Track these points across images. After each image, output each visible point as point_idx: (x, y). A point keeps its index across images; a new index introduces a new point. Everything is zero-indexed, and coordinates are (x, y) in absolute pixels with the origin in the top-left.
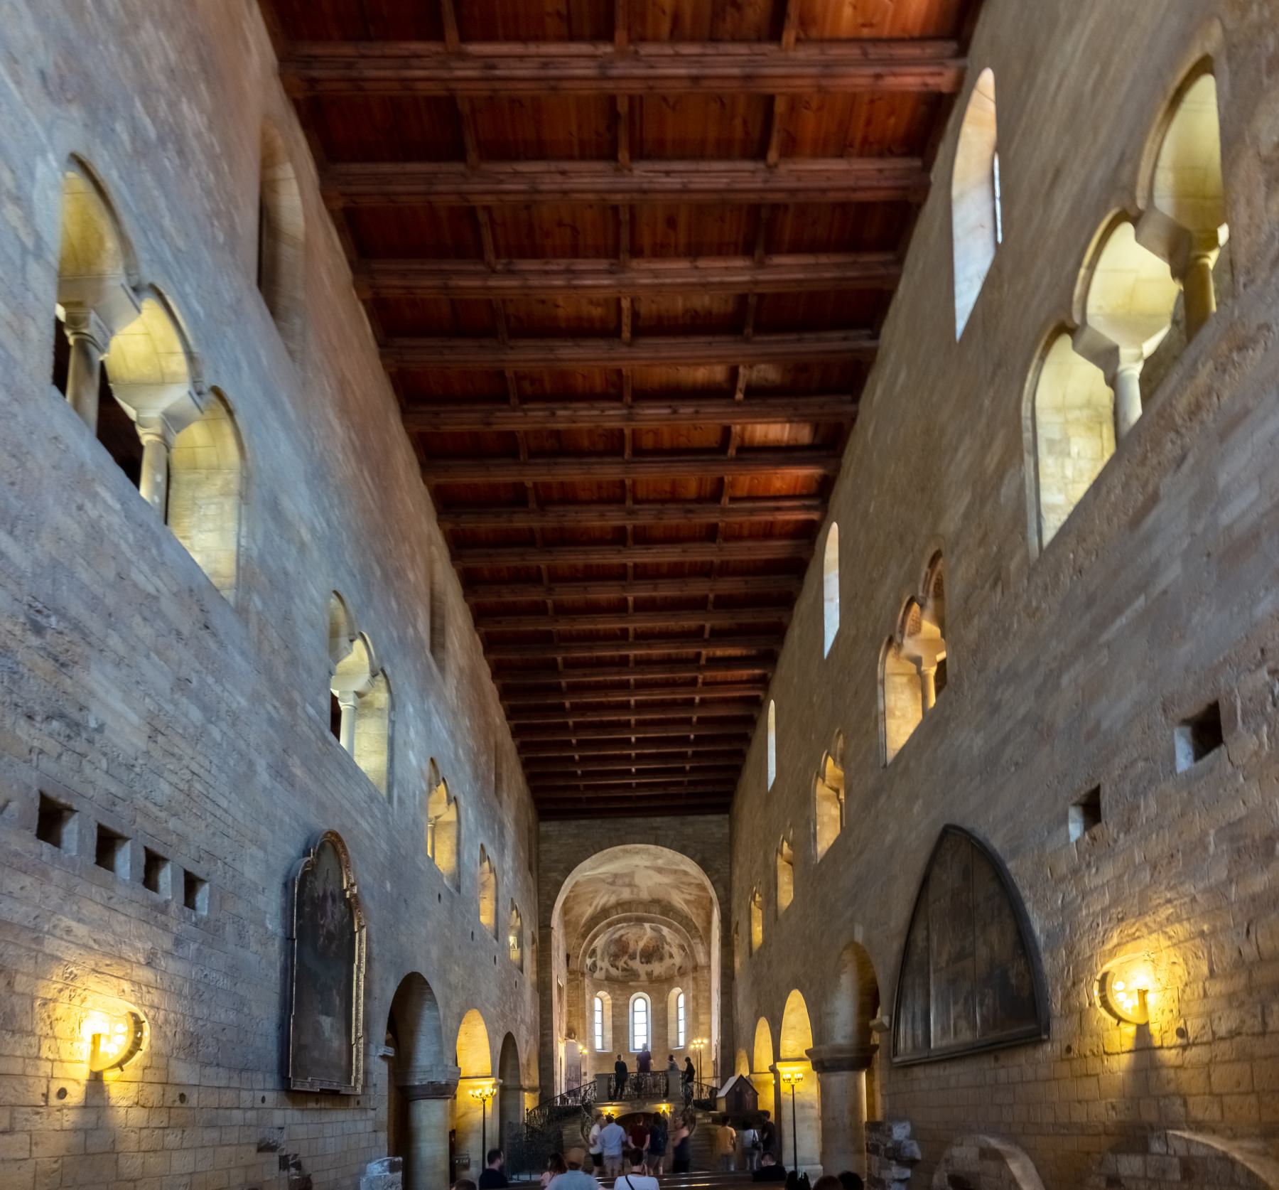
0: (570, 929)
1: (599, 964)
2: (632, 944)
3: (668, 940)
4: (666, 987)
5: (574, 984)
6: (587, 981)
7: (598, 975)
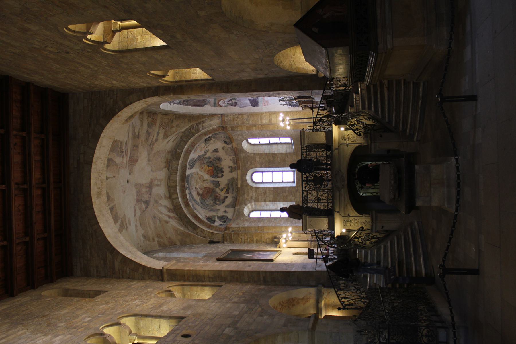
1: (220, 214)
2: (205, 185)
3: (202, 153)
4: (242, 155)
5: (234, 237)
6: (234, 225)
7: (230, 215)
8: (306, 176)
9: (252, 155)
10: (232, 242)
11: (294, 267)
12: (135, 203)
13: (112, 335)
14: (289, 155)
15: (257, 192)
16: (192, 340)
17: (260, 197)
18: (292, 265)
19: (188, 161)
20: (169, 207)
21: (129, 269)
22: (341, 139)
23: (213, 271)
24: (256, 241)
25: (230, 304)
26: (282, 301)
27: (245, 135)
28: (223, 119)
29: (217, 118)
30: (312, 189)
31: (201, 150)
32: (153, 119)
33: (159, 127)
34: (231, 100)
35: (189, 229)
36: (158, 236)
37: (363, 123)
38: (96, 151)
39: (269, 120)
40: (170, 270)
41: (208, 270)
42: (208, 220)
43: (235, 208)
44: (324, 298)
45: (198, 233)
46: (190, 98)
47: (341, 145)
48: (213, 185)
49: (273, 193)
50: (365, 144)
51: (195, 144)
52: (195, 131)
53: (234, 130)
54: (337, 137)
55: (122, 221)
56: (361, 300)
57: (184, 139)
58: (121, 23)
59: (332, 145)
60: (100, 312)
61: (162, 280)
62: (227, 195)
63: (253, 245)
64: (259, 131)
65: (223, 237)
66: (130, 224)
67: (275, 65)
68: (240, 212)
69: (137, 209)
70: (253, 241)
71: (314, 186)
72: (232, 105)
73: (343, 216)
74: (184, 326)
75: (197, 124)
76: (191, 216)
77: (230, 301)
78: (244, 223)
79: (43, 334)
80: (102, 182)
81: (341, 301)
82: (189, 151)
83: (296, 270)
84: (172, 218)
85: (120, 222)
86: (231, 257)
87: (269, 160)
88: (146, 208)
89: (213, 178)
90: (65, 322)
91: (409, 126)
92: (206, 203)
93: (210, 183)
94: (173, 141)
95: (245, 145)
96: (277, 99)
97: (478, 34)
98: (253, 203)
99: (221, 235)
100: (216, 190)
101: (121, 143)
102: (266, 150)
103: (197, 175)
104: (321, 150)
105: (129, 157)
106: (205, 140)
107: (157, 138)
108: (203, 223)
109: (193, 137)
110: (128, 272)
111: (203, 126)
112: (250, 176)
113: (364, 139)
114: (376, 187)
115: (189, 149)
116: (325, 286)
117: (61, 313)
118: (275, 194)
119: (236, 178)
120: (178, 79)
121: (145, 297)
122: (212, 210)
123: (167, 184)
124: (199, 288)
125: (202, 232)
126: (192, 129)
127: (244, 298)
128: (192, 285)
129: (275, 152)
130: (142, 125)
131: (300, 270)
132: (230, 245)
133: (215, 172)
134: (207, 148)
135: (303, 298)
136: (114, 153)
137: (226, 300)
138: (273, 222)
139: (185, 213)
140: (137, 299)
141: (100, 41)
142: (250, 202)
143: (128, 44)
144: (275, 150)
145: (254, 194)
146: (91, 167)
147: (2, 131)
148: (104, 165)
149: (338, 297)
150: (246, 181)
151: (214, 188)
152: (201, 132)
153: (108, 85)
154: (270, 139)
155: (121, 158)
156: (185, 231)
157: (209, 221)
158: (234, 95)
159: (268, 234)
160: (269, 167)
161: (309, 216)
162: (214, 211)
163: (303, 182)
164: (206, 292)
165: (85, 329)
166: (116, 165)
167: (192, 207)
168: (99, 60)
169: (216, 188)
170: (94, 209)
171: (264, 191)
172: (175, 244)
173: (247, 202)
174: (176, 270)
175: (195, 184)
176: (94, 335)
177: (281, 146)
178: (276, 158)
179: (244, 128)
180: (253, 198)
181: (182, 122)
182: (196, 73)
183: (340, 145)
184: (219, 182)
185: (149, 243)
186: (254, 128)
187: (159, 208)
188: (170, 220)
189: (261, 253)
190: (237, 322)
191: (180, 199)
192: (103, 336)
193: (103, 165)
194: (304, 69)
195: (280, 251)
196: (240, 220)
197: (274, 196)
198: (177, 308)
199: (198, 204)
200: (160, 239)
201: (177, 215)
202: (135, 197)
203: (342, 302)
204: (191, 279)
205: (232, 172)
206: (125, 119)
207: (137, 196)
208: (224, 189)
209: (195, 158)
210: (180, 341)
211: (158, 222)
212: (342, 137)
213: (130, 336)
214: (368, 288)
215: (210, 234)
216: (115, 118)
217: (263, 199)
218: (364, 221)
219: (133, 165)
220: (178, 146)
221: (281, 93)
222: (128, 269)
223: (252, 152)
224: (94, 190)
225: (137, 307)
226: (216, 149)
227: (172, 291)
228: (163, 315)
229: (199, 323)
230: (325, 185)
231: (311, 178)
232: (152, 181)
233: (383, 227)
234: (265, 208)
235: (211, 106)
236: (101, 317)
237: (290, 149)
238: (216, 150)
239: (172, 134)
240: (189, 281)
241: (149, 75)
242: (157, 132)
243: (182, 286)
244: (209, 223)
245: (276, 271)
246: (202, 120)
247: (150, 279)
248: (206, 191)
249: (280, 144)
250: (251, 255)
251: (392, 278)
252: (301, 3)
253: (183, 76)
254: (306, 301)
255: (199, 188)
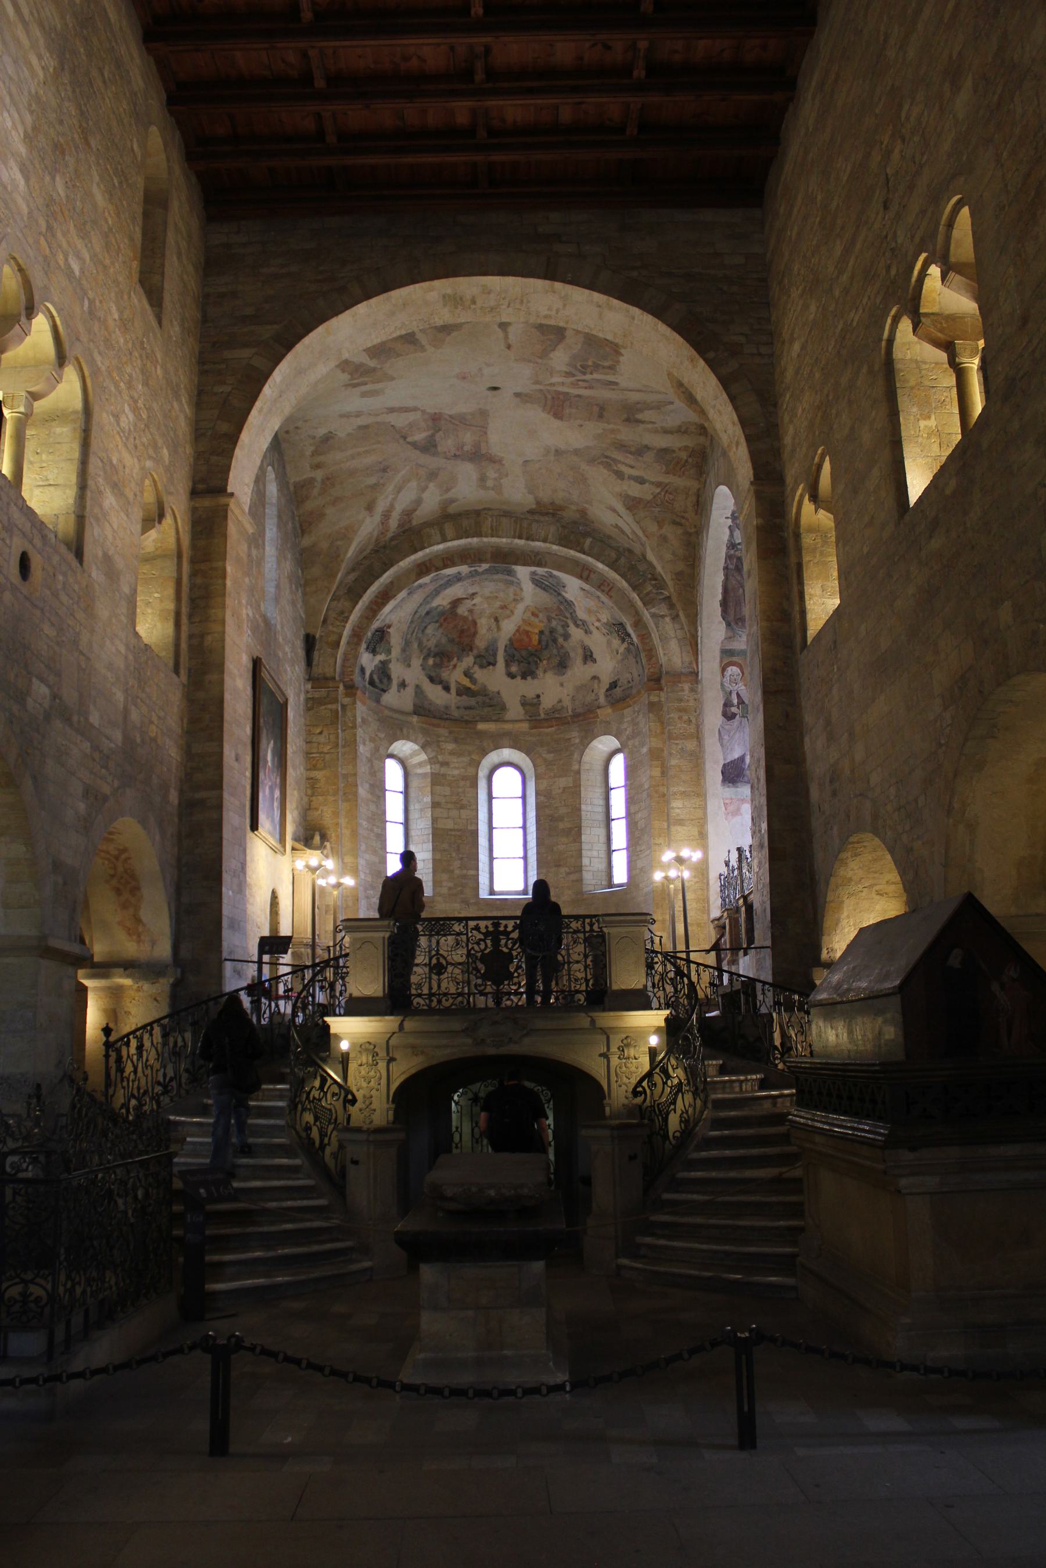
0: (316, 571)
1: (396, 670)
2: (484, 624)
3: (581, 614)
4: (575, 735)
5: (324, 710)
6: (361, 710)
7: (391, 698)
8: (510, 929)
9: (576, 767)
10: (312, 704)
11: (233, 892)
12: (428, 411)
13: (28, 339)
14: (573, 877)
15: (463, 780)
16: (12, 584)
17: (447, 791)
18: (242, 886)
19: (555, 573)
20: (417, 513)
21: (230, 392)
22: (625, 1036)
23: (223, 647)
24: (312, 778)
25: (122, 699)
26: (129, 858)
27: (637, 744)
28: (683, 678)
29: (688, 658)
30: (473, 948)
31: (589, 611)
32: (684, 466)
33: (658, 484)
34: (741, 702)
35: (348, 573)
36: (328, 479)
37: (671, 1103)
38: (587, 292)
39: (682, 817)
40: (226, 517)
41: (224, 632)
42: (377, 631)
43: (415, 713)
44: (140, 984)
45: (339, 600)
46: (749, 577)
47: (605, 1036)
48: (483, 647)
49: (458, 830)
50: (607, 1109)
51: (607, 594)
52: (648, 594)
53: (650, 711)
54: (629, 1025)
55: (374, 370)
56: (133, 1096)
57: (623, 560)
58: (975, 367)
59: (604, 1010)
60: (98, 303)
61: (194, 493)
62: (453, 691)
63: (302, 768)
64: (646, 786)
65: (326, 679)
66: (364, 395)
67: (848, 837)
68: (401, 730)
69: (412, 417)
70: (314, 768)
71: (479, 955)
72: (727, 704)
73: (391, 1042)
74: (56, 559)
75: (668, 598)
76: (388, 581)
77: (130, 698)
78: (367, 743)
79: (30, 130)
80: (492, 309)
81: (131, 1037)
82: (585, 574)
83: (225, 901)
84: (383, 523)
85: (372, 363)
86: (264, 701)
87: (561, 819)
88: (415, 445)
89: (506, 646)
90: (67, 196)
91: (662, 1242)
92: (429, 627)
93: (490, 637)
94: (617, 526)
95: (605, 743)
96: (746, 841)
97: (942, 1452)
98: (427, 769)
99: (332, 670)
100: (468, 655)
101: (610, 368)
102: (591, 808)
103: (515, 600)
104: (589, 977)
105: (567, 393)
106: (621, 624)
107: (626, 476)
108: (367, 618)
109: (630, 585)
110: (219, 389)
111: (663, 616)
112: (511, 760)
113: (624, 1105)
114: (477, 1142)
115: (592, 576)
116: (175, 986)
117: (95, 185)
118: (455, 836)
119: (506, 719)
120: (807, 540)
121: (144, 440)
122: (407, 644)
123: (487, 506)
124: (171, 606)
125: (342, 613)
126: (654, 582)
127: (138, 740)
128: (179, 583)
129: (583, 837)
130: (666, 431)
131: (226, 911)
132: (302, 697)
133: (524, 653)
134: (597, 628)
135: (138, 921)
136: (579, 346)
137: (133, 687)
138: (372, 830)
139: (398, 562)
140: (138, 417)
141: (922, 304)
142: (432, 758)
143: (912, 388)
144: (592, 835)
145: (456, 772)
146: (539, 277)
147: (647, 5)
148: (546, 317)
149: (144, 1027)
150: (496, 748)
151: (475, 652)
152: (646, 611)
153: (786, 327)
154: (624, 820)
155: (564, 369)
156: (342, 561)
157: (374, 635)
158: (758, 710)
159: (336, 814)
160: (537, 816)
161: (389, 938)
162: (404, 650)
163: (491, 922)
164: (159, 625)
165: (45, 257)
166: (544, 354)
167: (416, 584)
168: (865, 300)
169: (476, 657)
170: (411, 287)
171: (464, 802)
172: (303, 532)
173: (433, 751)
174: (225, 536)
175: (487, 592)
176: (27, 284)
177: (603, 854)
178: (564, 840)
179: (655, 743)
180: (443, 770)
181: (674, 554)
182: (822, 596)
183: (606, 1034)
184: (494, 664)
185: (308, 453)
186: (657, 772)
187: (414, 484)
188: (377, 518)
189: (277, 793)
190: (68, 720)
191: (441, 547)
192: (23, 313)
193: (546, 312)
194: (837, 924)
195: (282, 849)
196: (378, 730)
197: (450, 833)
198: (110, 537)
199: (426, 601)
200: (318, 485)
201: (392, 539)
202: (448, 411)
203: (129, 1041)
204: (199, 581)
205: (524, 704)
206: (685, 381)
207: (450, 416)
208: (471, 681)
209: (566, 592)
210: (10, 547)
211: (372, 480)
212: (630, 1039)
213: (24, 394)
214: (172, 1118)
215: (333, 638)
216: (688, 350)
217: (443, 801)
218: (373, 1107)
219: (545, 405)
220: (601, 541)
221: (764, 853)
222: (227, 389)
223: (584, 767)
224: (468, 285)
225: (113, 415)
226: (594, 656)
227: (160, 522)
228: (89, 494)
229: (63, 604)
230: (483, 987)
231: (506, 945)
232: (494, 462)
233: (355, 1162)
234: (414, 807)
235: (722, 643)
236: (82, 306)
237: (593, 882)
238: (591, 656)
239: (637, 522)
240: (193, 574)
241: (819, 452)
242: (646, 477)
243: (175, 552)
244: (369, 634)
245: (221, 838)
246: (681, 614)
247: (198, 456)
248: (465, 627)
249: (609, 852)
250: (270, 764)
251: (202, 1191)
252: (1037, 915)
253: (815, 557)
254: (129, 929)
255: (474, 605)
